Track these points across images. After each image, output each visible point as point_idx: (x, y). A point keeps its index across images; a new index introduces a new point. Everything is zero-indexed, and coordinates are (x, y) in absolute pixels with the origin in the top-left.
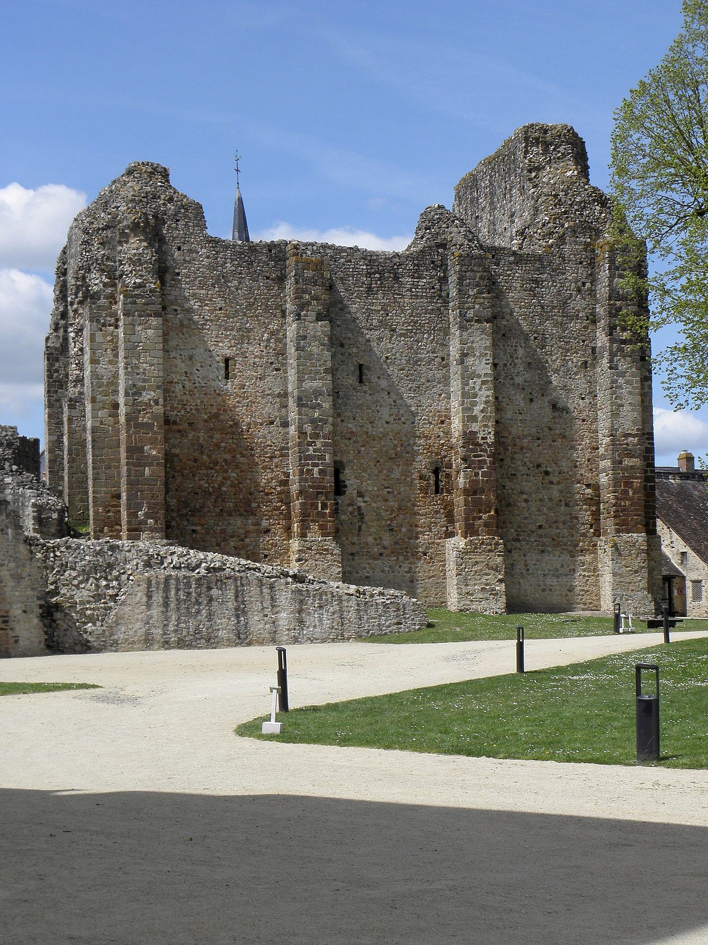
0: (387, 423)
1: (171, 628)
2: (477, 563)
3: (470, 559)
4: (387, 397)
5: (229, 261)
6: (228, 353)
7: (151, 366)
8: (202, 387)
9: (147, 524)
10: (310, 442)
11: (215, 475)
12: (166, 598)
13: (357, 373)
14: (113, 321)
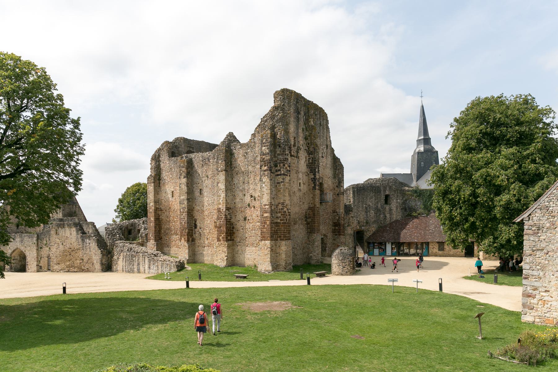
1: (127, 267)
2: (220, 250)
6: (172, 190)
13: (200, 192)
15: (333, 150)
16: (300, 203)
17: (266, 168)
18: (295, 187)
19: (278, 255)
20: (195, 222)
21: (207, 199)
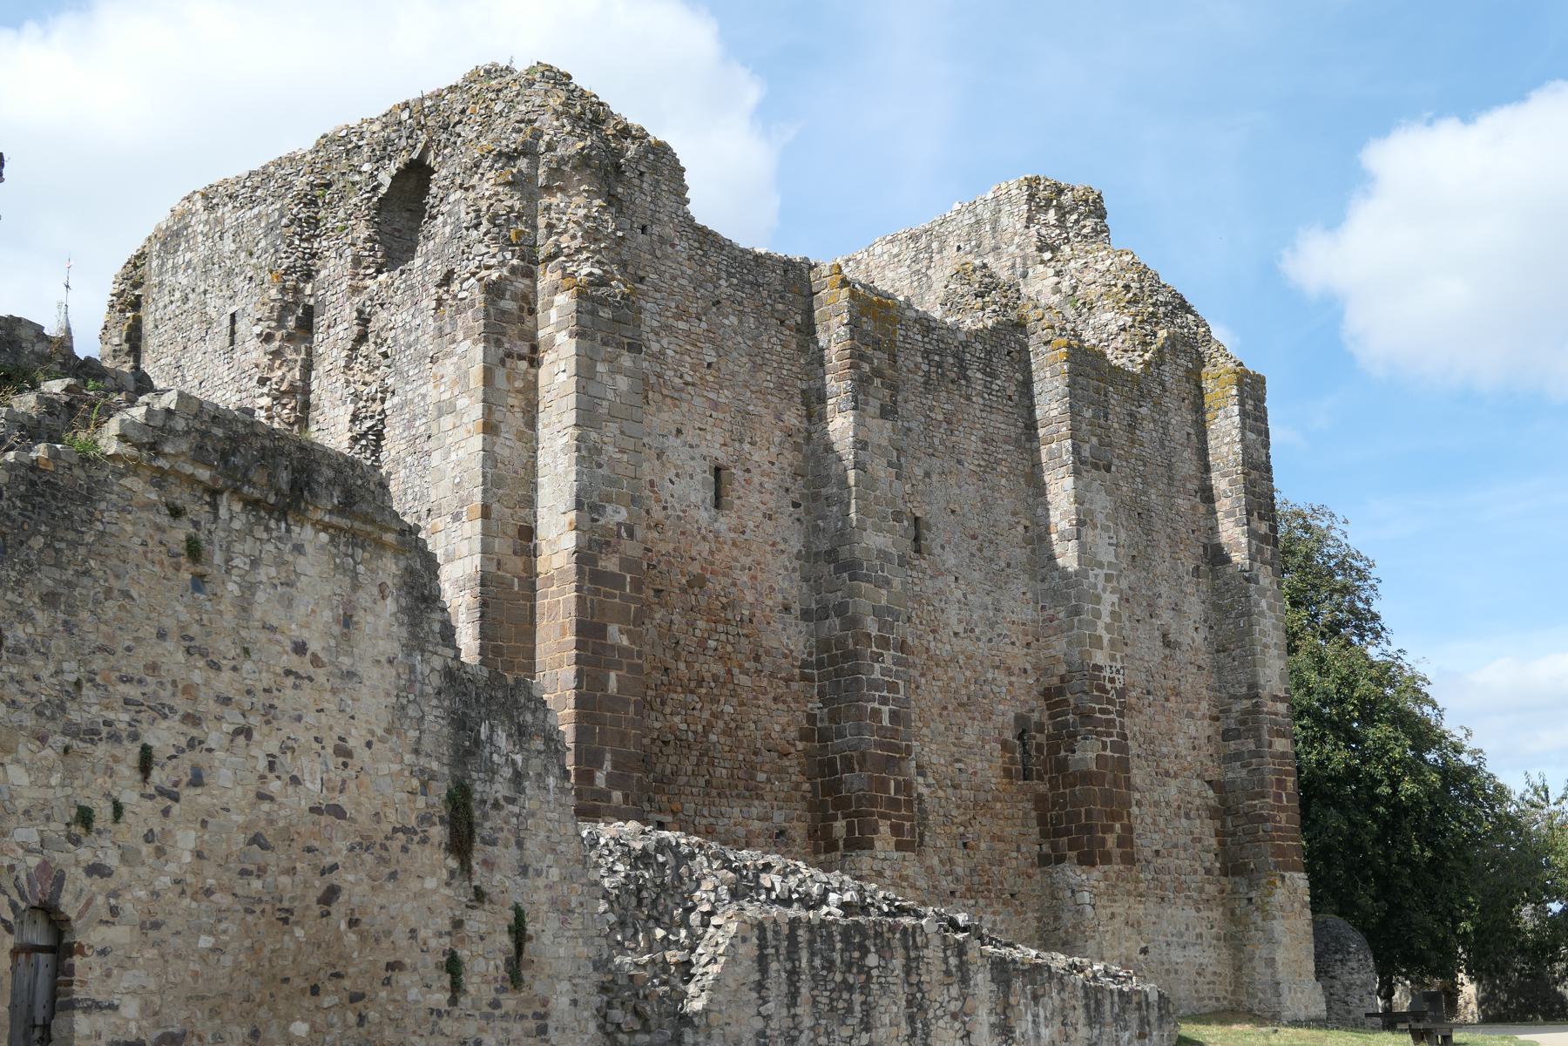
0: (956, 634)
2: (1113, 916)
3: (1104, 907)
4: (953, 585)
5: (724, 275)
7: (622, 451)
8: (679, 518)
9: (609, 799)
10: (876, 653)
11: (699, 706)
12: (793, 974)
13: (912, 533)
14: (525, 349)
21: (958, 594)
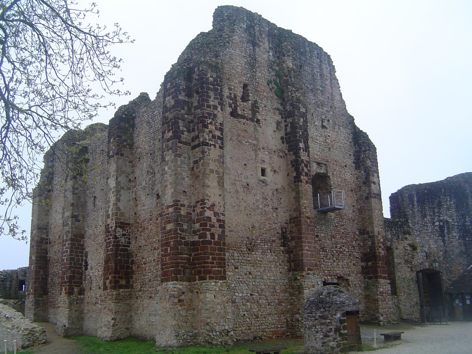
15: (351, 119)
16: (266, 209)
17: (170, 134)
18: (250, 177)
19: (196, 312)
20: (86, 257)
